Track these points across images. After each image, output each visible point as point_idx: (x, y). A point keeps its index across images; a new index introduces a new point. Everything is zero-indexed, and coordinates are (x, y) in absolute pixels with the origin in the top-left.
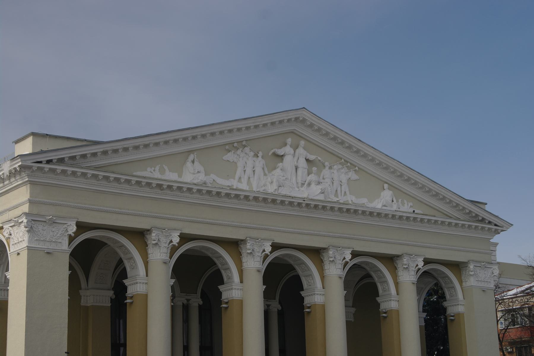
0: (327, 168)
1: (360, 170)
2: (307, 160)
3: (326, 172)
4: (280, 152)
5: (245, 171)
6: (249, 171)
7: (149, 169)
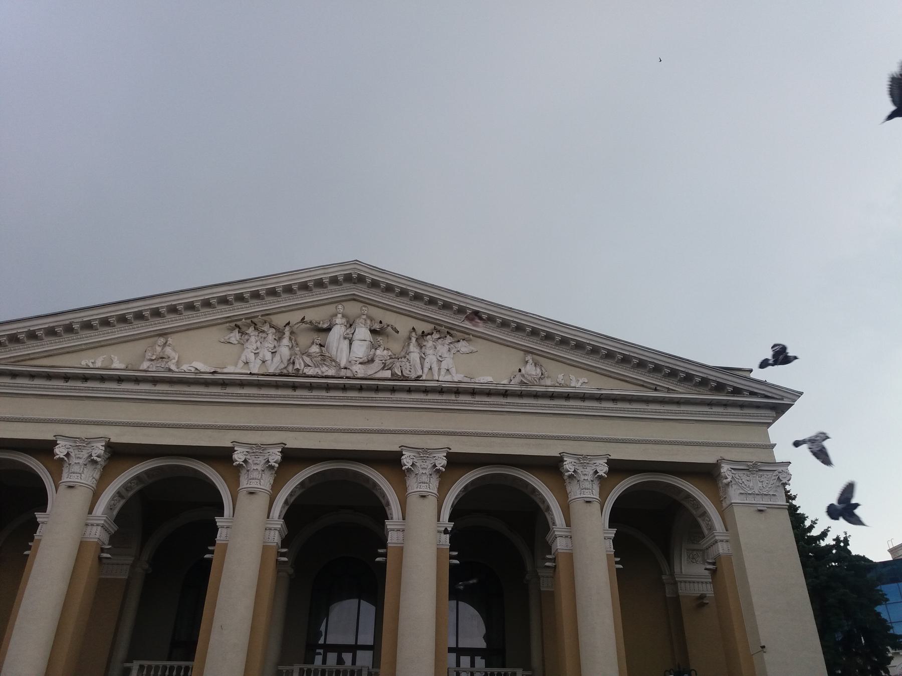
2: (373, 332)
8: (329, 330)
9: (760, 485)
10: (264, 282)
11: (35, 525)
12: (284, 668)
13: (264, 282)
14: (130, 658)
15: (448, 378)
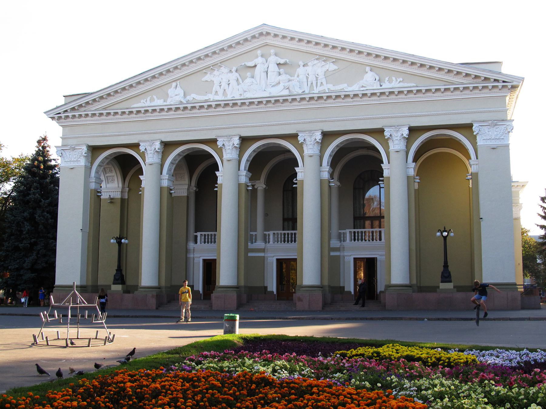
0: (301, 66)
1: (336, 60)
3: (301, 71)
4: (251, 64)
5: (220, 86)
6: (224, 85)
7: (142, 101)
8: (255, 66)
9: (496, 133)
10: (218, 46)
11: (140, 181)
12: (267, 233)
13: (218, 46)
14: (196, 232)
15: (320, 89)
